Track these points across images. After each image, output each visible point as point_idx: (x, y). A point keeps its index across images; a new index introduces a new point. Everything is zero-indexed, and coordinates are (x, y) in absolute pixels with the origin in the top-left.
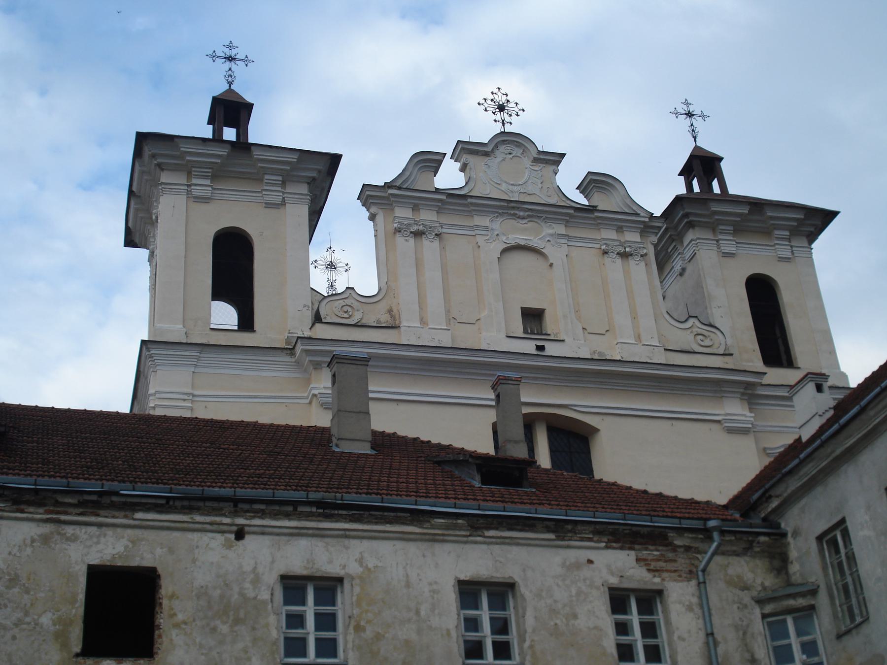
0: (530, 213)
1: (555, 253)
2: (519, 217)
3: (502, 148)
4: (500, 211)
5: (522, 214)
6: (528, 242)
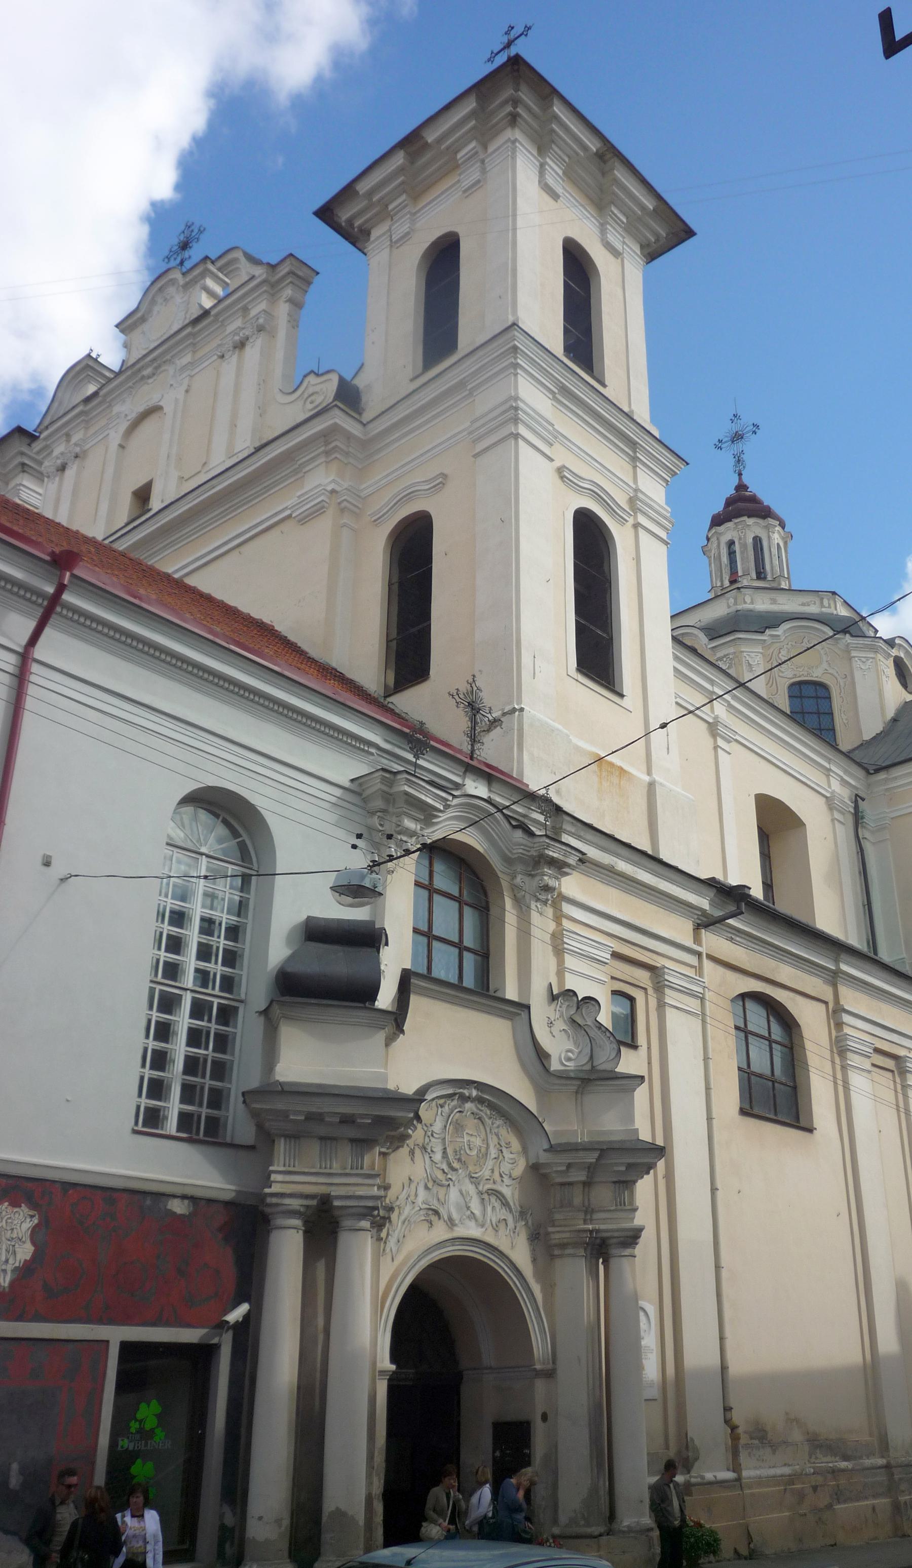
0: (155, 364)
2: (149, 377)
3: (159, 300)
4: (130, 384)
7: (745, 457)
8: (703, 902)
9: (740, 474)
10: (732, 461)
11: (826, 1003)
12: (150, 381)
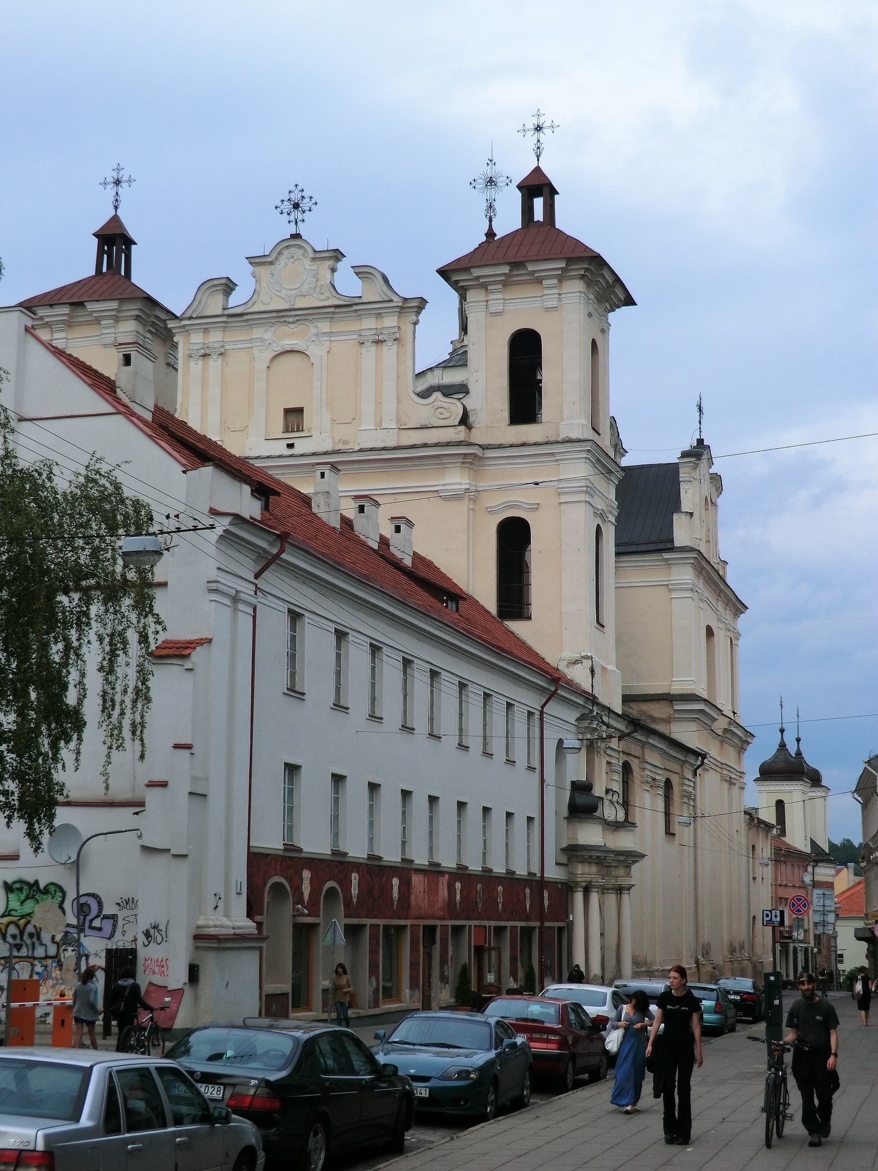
1: (316, 352)
2: (289, 323)
3: (286, 253)
4: (273, 321)
5: (291, 320)
6: (294, 346)
7: (496, 205)
8: (621, 726)
9: (491, 221)
10: (485, 205)
11: (639, 758)
12: (292, 326)
